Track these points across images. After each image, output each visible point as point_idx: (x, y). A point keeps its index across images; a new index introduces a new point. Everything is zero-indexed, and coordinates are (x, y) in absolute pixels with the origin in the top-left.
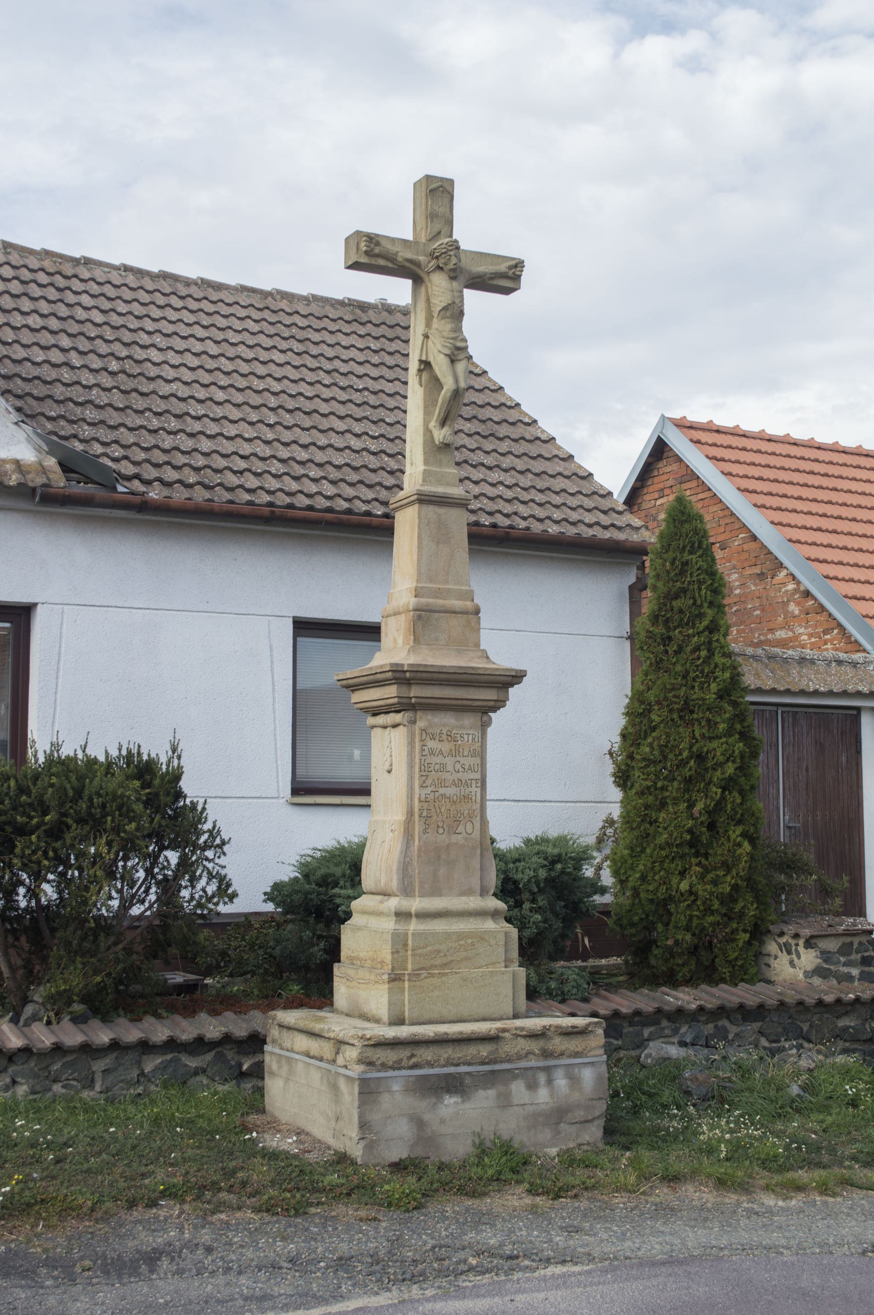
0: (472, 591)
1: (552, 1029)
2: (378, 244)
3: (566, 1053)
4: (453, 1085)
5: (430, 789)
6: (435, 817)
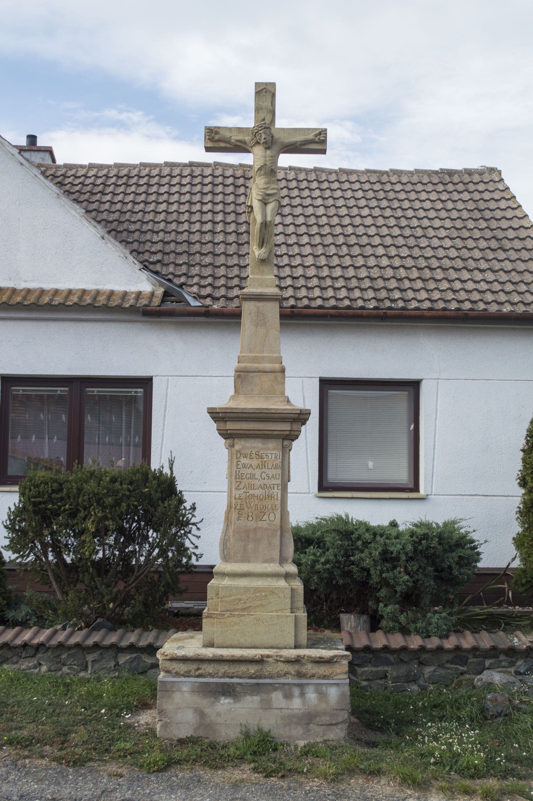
0: (281, 357)
1: (306, 658)
2: (217, 133)
3: (316, 675)
4: (227, 691)
5: (242, 491)
6: (246, 510)
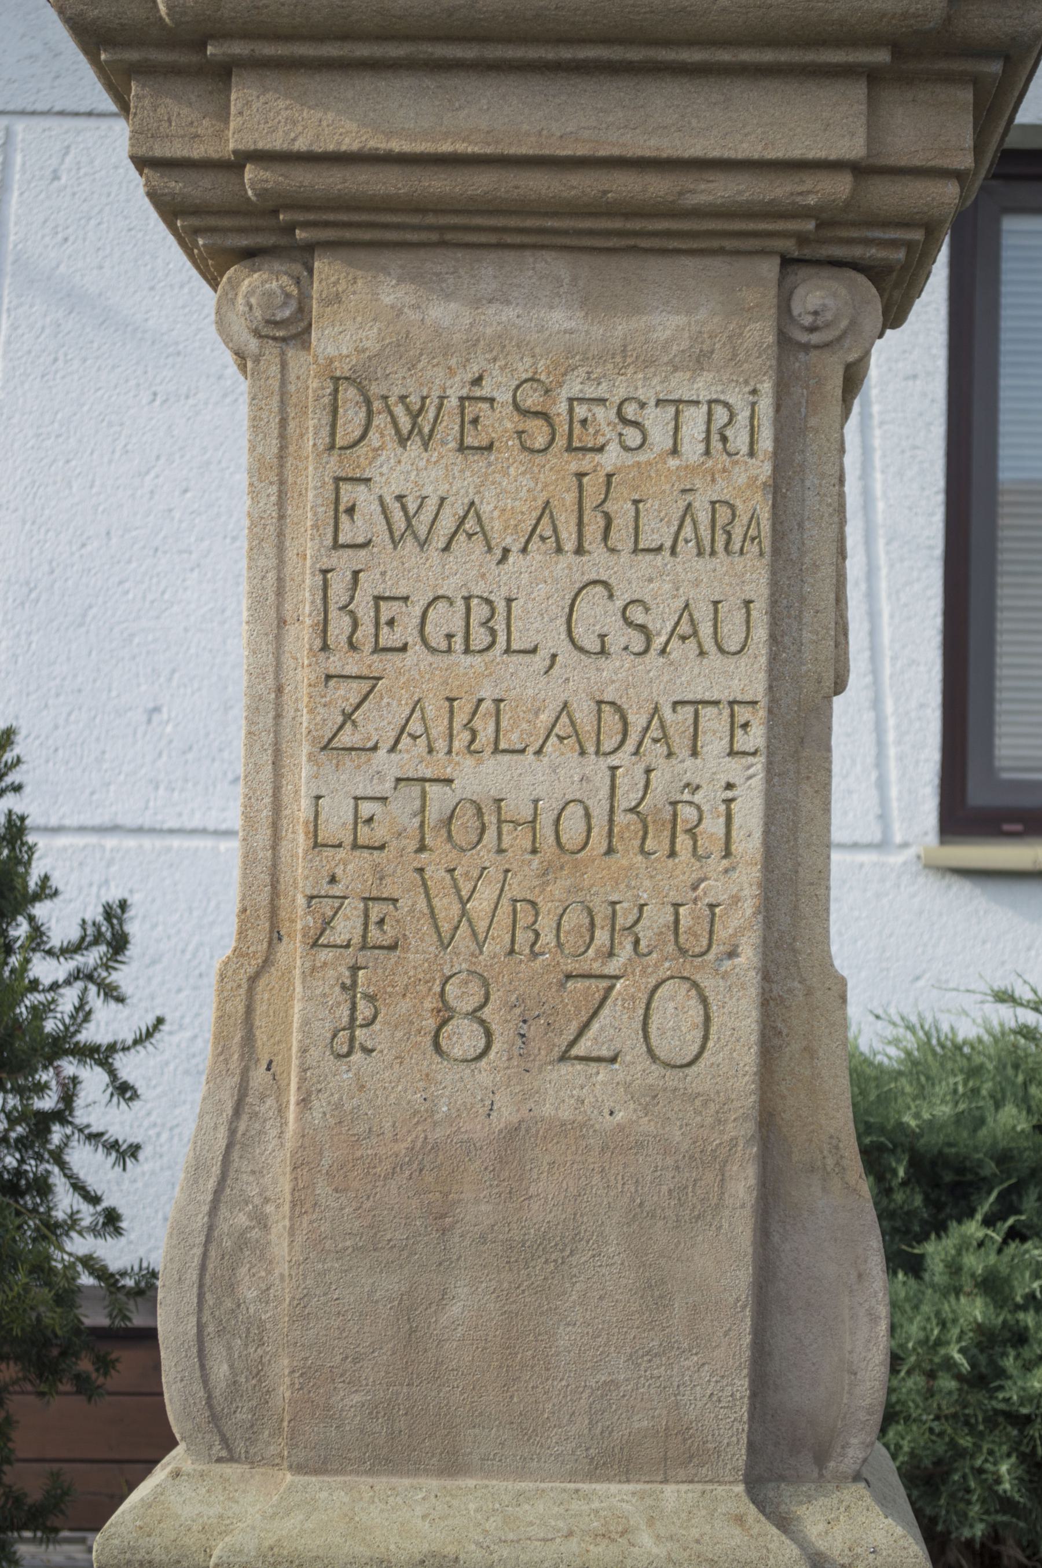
6: (420, 950)
